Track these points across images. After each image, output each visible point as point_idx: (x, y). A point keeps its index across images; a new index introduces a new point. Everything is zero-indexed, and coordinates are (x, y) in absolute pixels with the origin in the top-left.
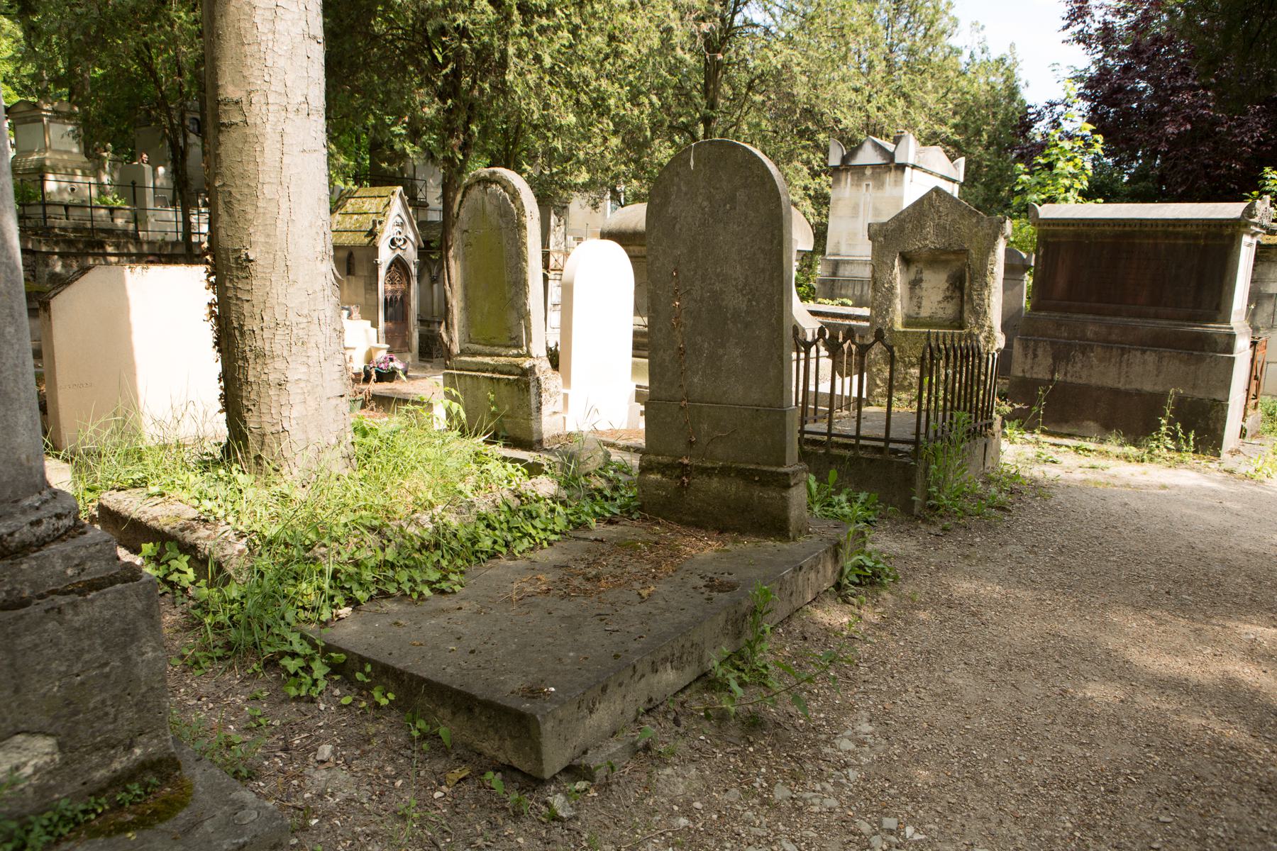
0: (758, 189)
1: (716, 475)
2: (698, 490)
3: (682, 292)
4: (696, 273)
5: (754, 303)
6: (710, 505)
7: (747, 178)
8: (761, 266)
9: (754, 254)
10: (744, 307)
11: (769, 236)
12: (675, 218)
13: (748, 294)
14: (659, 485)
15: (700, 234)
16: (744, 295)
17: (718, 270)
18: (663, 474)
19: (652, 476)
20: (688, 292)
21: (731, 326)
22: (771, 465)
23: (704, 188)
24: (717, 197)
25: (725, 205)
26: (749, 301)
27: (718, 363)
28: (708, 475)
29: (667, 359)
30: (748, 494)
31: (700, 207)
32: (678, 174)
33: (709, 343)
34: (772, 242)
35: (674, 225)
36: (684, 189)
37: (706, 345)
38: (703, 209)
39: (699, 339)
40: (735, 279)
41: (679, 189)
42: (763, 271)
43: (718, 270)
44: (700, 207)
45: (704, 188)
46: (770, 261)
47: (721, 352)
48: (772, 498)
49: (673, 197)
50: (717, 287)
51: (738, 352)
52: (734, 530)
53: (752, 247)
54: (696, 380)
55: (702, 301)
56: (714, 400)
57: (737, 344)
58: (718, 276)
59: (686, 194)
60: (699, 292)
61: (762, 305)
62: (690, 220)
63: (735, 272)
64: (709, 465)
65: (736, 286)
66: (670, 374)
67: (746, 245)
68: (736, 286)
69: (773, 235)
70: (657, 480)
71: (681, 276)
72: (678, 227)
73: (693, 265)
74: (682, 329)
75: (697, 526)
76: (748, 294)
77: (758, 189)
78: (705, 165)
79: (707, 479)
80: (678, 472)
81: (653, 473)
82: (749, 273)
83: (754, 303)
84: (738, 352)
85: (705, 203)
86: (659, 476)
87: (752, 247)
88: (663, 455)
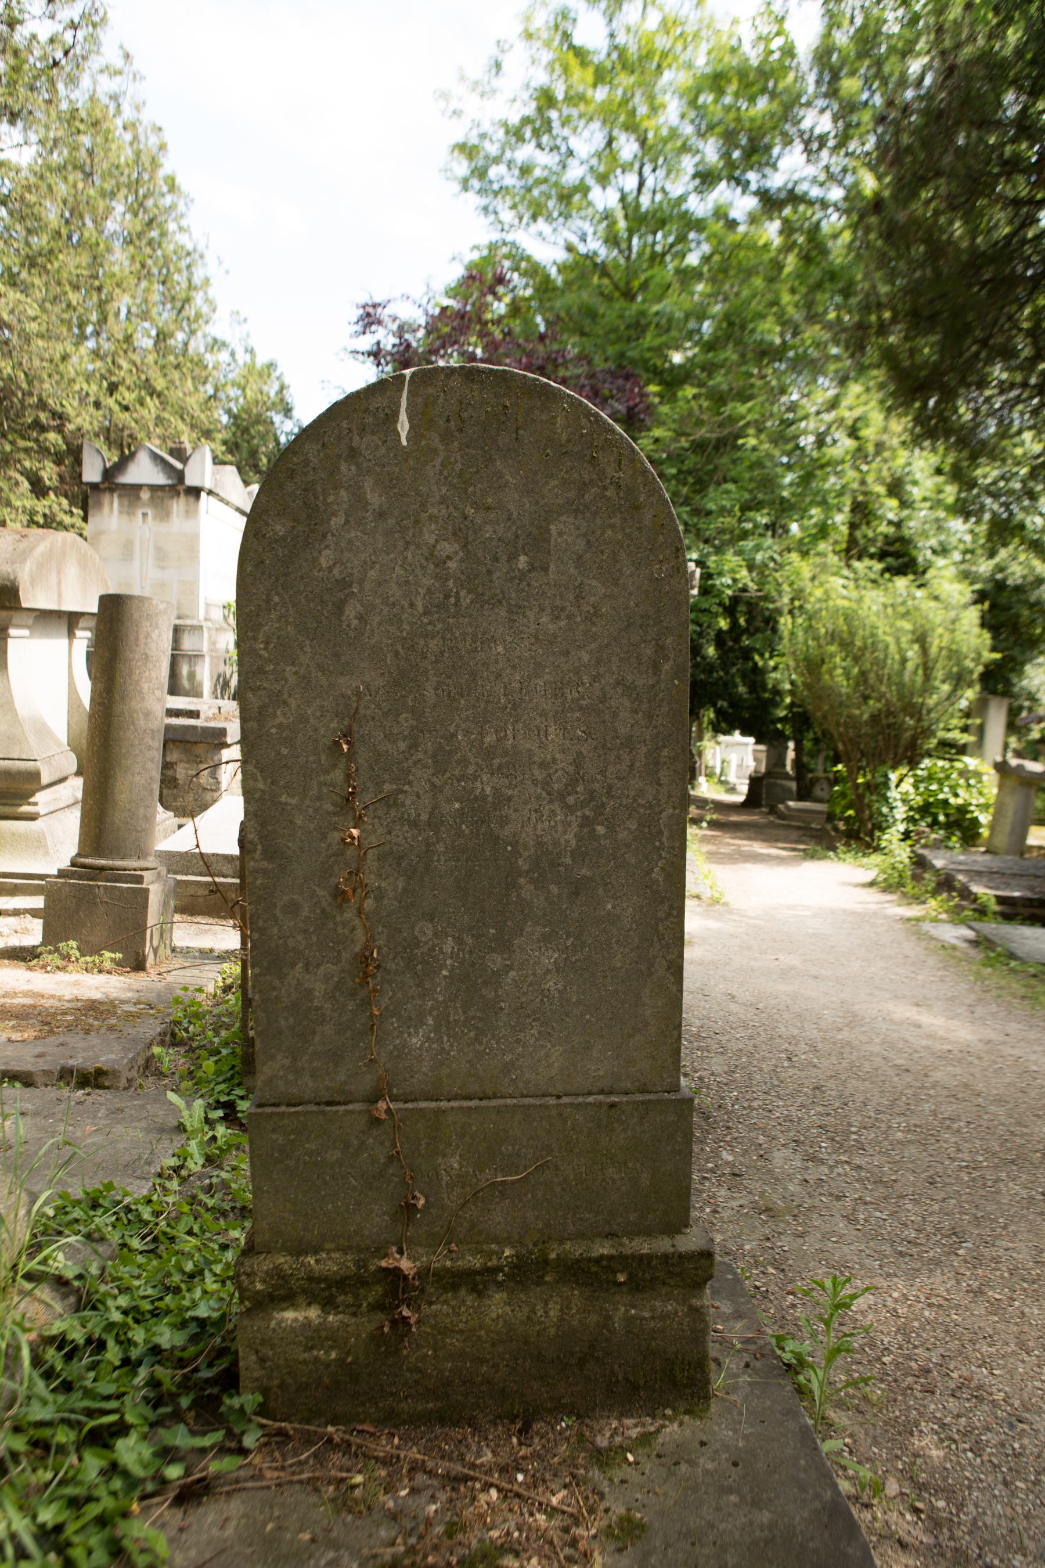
0: (617, 520)
1: (499, 1285)
2: (445, 1331)
3: (368, 798)
4: (414, 746)
5: (600, 830)
6: (481, 1361)
7: (583, 487)
8: (623, 731)
9: (604, 698)
10: (570, 838)
11: (648, 651)
12: (344, 584)
13: (584, 804)
14: (313, 1336)
15: (428, 636)
16: (570, 809)
17: (490, 739)
18: (328, 1304)
19: (290, 1315)
20: (389, 801)
21: (527, 890)
22: (648, 1233)
23: (443, 501)
24: (488, 532)
25: (513, 557)
26: (586, 822)
27: (488, 993)
28: (474, 1289)
29: (320, 989)
30: (594, 1318)
31: (431, 556)
32: (353, 454)
33: (459, 941)
34: (656, 668)
35: (340, 607)
36: (375, 499)
37: (449, 945)
38: (441, 563)
39: (428, 930)
40: (543, 765)
41: (359, 500)
42: (629, 743)
43: (490, 739)
44: (431, 556)
45: (443, 501)
46: (649, 716)
47: (495, 961)
48: (664, 1317)
49: (337, 522)
50: (486, 785)
51: (550, 958)
52: (560, 1409)
53: (595, 679)
54: (415, 1041)
55: (435, 823)
56: (474, 1088)
57: (546, 938)
58: (488, 754)
59: (381, 515)
60: (426, 799)
61: (622, 835)
62: (394, 591)
63: (542, 746)
64: (476, 1262)
65: (546, 784)
66: (328, 1029)
67: (577, 672)
68: (546, 784)
69: (660, 648)
70: (307, 1324)
71: (363, 756)
72: (351, 611)
73: (406, 721)
74: (369, 904)
75: (442, 1421)
76: (584, 804)
77: (617, 520)
78: (446, 437)
79: (470, 1300)
80: (376, 1292)
81: (295, 1306)
82: (585, 749)
83: (600, 830)
84: (550, 958)
85: (447, 548)
86: (313, 1313)
87: (595, 679)
88: (315, 1252)
